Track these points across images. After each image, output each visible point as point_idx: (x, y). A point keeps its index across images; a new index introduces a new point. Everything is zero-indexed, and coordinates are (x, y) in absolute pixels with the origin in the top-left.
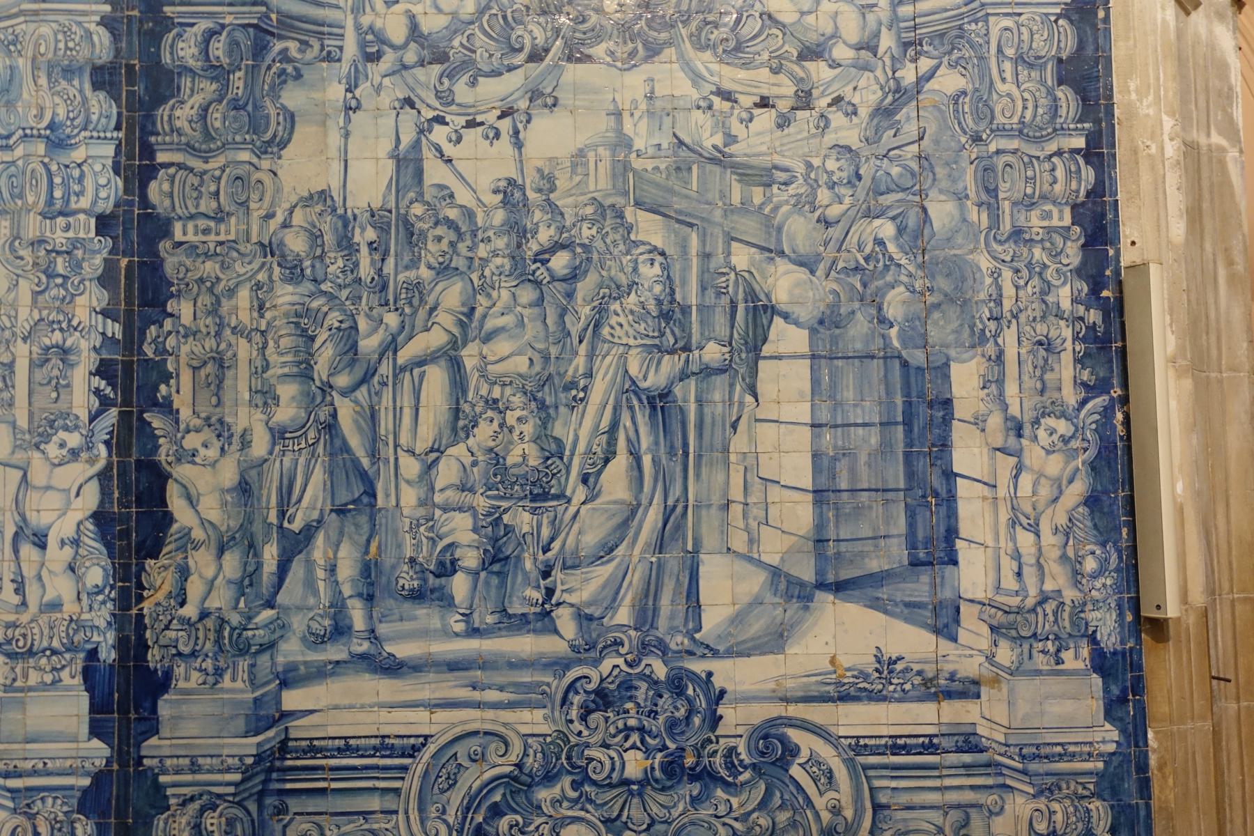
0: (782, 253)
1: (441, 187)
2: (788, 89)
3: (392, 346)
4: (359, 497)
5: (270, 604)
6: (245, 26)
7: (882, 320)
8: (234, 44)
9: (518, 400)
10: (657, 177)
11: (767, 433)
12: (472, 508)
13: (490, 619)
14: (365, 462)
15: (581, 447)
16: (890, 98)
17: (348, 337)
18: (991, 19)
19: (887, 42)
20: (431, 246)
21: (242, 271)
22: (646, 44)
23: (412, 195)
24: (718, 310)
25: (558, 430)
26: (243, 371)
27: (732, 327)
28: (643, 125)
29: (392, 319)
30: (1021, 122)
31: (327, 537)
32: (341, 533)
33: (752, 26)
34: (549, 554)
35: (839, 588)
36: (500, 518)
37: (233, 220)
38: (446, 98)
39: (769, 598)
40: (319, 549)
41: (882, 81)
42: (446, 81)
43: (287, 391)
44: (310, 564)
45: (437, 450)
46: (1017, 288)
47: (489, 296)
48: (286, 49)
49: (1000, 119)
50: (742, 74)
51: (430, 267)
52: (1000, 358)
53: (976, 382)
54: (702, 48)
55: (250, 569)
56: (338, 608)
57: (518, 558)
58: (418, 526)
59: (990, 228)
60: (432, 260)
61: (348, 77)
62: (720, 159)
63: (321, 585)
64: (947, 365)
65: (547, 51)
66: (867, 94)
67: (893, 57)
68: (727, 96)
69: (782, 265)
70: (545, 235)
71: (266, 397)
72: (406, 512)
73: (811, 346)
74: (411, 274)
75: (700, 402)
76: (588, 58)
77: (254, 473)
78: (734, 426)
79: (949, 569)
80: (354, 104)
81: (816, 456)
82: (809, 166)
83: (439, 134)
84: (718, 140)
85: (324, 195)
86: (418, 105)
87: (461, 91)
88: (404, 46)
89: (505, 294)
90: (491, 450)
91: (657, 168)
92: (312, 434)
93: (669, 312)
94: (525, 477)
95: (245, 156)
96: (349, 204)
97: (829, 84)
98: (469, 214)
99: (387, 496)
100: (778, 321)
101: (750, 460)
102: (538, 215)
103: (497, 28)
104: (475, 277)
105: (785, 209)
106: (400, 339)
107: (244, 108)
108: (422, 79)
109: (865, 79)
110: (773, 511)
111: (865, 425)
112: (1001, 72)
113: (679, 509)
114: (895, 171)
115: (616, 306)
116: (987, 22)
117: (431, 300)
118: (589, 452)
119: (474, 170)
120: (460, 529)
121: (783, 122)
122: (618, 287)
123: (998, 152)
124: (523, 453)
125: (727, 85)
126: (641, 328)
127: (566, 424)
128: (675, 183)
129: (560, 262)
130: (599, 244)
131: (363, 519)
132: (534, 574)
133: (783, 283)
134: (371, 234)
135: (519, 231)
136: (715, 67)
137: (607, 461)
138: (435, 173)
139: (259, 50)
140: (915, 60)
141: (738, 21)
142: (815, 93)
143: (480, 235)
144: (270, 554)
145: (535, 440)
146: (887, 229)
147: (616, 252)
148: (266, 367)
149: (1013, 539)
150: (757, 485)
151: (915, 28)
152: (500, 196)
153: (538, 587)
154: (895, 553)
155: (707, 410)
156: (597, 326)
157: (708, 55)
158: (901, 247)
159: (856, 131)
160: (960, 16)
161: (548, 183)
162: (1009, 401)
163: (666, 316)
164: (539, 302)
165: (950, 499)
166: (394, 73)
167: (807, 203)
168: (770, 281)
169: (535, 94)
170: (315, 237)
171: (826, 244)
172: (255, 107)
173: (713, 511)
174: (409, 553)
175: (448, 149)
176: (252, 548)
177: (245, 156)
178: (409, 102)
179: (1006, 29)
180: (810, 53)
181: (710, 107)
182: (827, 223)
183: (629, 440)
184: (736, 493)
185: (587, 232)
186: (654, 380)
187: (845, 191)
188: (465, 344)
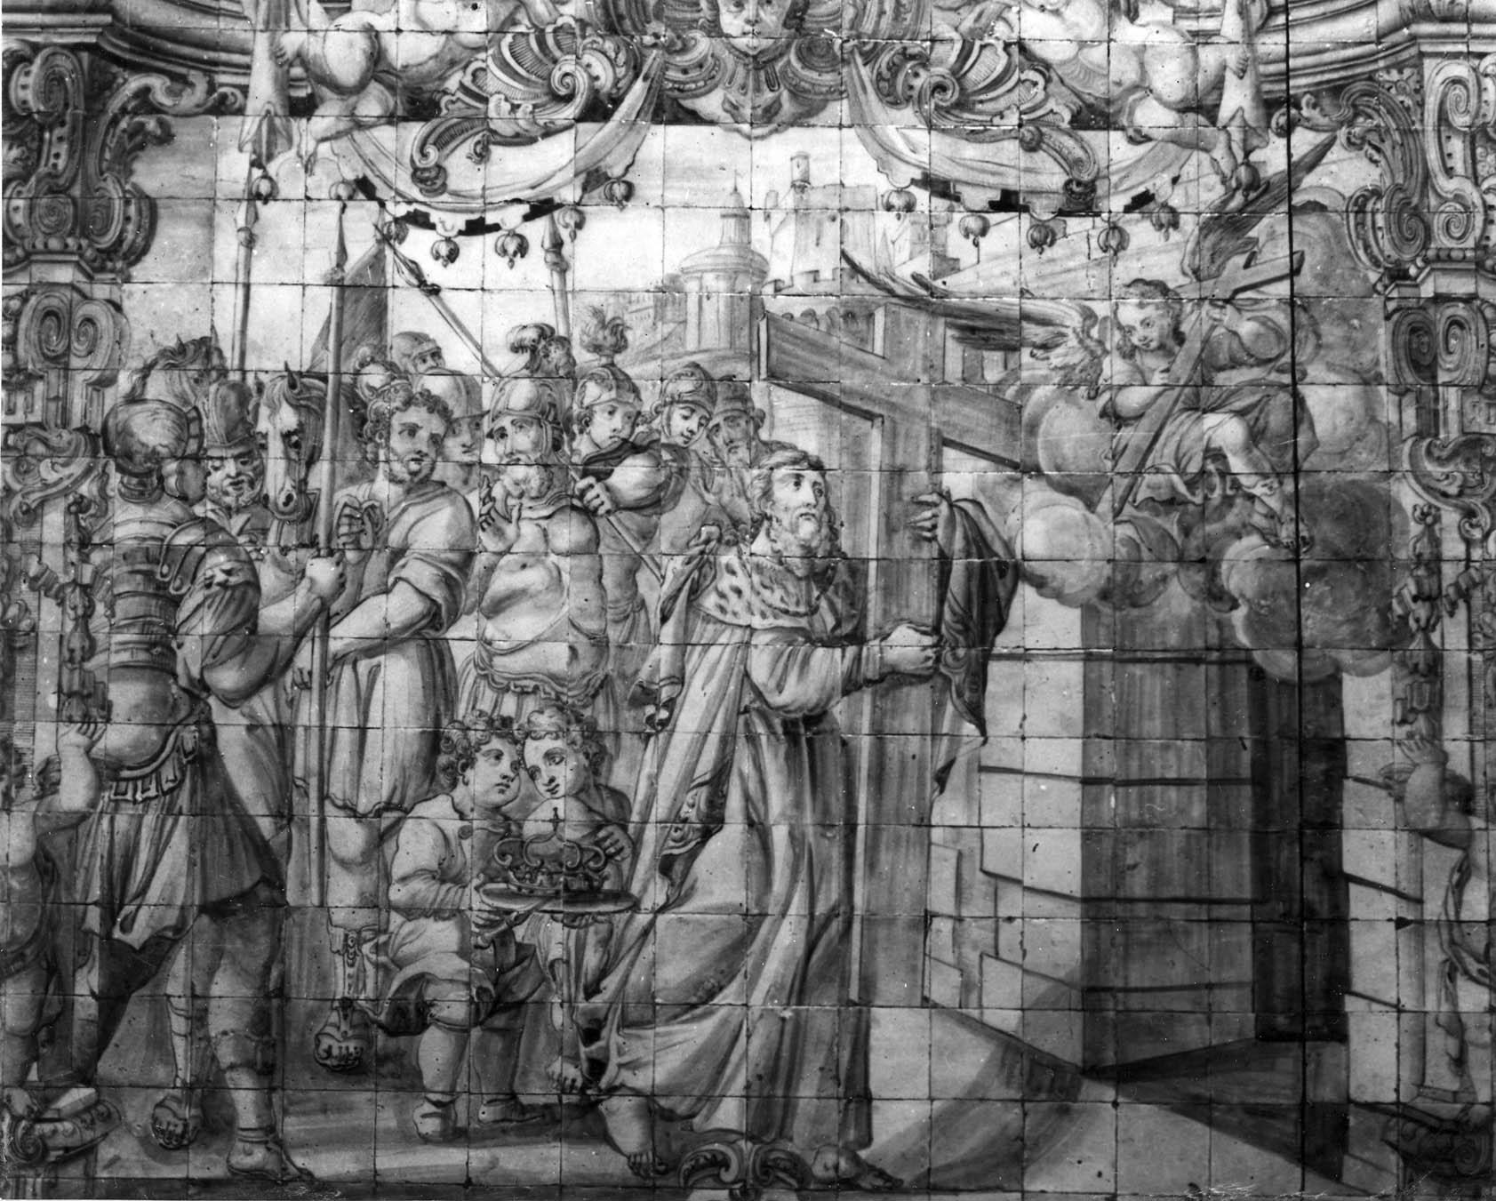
0: (1035, 471)
1: (418, 338)
2: (1053, 177)
3: (323, 616)
4: (250, 893)
5: (85, 1077)
6: (75, 48)
7: (1215, 594)
8: (53, 80)
9: (545, 721)
10: (810, 330)
11: (1000, 799)
12: (456, 913)
13: (486, 1114)
14: (266, 825)
15: (660, 809)
16: (1238, 200)
17: (243, 597)
18: (1428, 63)
19: (1236, 99)
20: (399, 443)
21: (52, 477)
22: (796, 93)
23: (364, 351)
24: (917, 567)
25: (619, 776)
26: (48, 659)
27: (942, 600)
28: (787, 237)
29: (322, 571)
30: (1477, 247)
31: (192, 958)
32: (219, 953)
33: (989, 64)
34: (598, 1000)
35: (1131, 1076)
36: (509, 933)
37: (39, 387)
38: (431, 179)
39: (997, 1090)
40: (177, 977)
41: (1225, 165)
42: (432, 151)
43: (126, 695)
44: (160, 1004)
45: (397, 808)
46: (1469, 543)
47: (499, 533)
48: (147, 90)
49: (1442, 241)
50: (971, 151)
51: (393, 479)
52: (1433, 668)
53: (1387, 712)
54: (893, 100)
55: (50, 1012)
56: (207, 1091)
57: (541, 1003)
58: (360, 942)
59: (1419, 435)
60: (397, 467)
61: (256, 141)
62: (925, 300)
63: (180, 1045)
64: (1335, 680)
65: (617, 102)
66: (1200, 188)
67: (1245, 127)
68: (941, 188)
69: (1035, 491)
70: (605, 429)
71: (87, 704)
72: (339, 916)
73: (1085, 635)
74: (360, 492)
75: (878, 734)
76: (694, 118)
77: (61, 840)
78: (941, 778)
79: (1330, 1051)
80: (264, 187)
81: (1090, 835)
82: (1089, 315)
83: (418, 245)
84: (923, 265)
85: (205, 347)
86: (382, 192)
87: (460, 167)
88: (360, 88)
89: (529, 531)
90: (497, 808)
91: (810, 314)
92: (168, 773)
93: (828, 571)
94: (556, 858)
95: (64, 274)
96: (251, 363)
97: (1128, 171)
98: (469, 388)
99: (304, 886)
100: (1026, 593)
101: (970, 840)
102: (592, 391)
103: (528, 60)
104: (474, 499)
105: (1040, 393)
106: (335, 607)
107: (64, 190)
108: (390, 146)
109: (1196, 163)
110: (1008, 934)
111: (1179, 782)
112: (1445, 156)
113: (836, 926)
114: (1247, 328)
115: (728, 557)
116: (1419, 67)
117: (395, 538)
118: (677, 819)
119: (480, 308)
120: (436, 946)
121: (1043, 239)
122: (736, 523)
123: (1440, 299)
124: (554, 814)
125: (943, 170)
126: (775, 597)
127: (636, 766)
128: (841, 340)
129: (631, 476)
130: (701, 446)
131: (260, 928)
132: (570, 1034)
133: (1038, 525)
134: (288, 418)
135: (557, 422)
136: (921, 136)
137: (706, 835)
138: (408, 312)
139: (98, 89)
140: (1286, 132)
141: (964, 55)
142: (1101, 187)
143: (486, 425)
144: (87, 983)
145: (579, 793)
146: (1226, 430)
147: (733, 460)
148: (90, 650)
149: (1452, 999)
150: (978, 886)
151: (1287, 75)
152: (524, 358)
153: (575, 1059)
154: (1236, 1015)
155: (892, 747)
156: (696, 592)
157: (907, 114)
158: (1252, 462)
159: (1177, 255)
160: (1370, 58)
161: (613, 336)
162: (1449, 746)
163: (820, 576)
164: (591, 547)
165: (1338, 923)
166: (337, 136)
167: (1082, 382)
168: (1013, 519)
169: (593, 178)
170: (186, 420)
171: (1116, 456)
172: (87, 188)
173: (900, 931)
174: (341, 989)
175: (435, 272)
176: (54, 976)
177: (64, 274)
178: (364, 187)
179: (1457, 81)
180: (1095, 115)
181: (909, 208)
182: (1115, 417)
183: (747, 798)
184: (941, 898)
185: (680, 424)
186: (796, 692)
187: (1153, 362)
188: (454, 617)
